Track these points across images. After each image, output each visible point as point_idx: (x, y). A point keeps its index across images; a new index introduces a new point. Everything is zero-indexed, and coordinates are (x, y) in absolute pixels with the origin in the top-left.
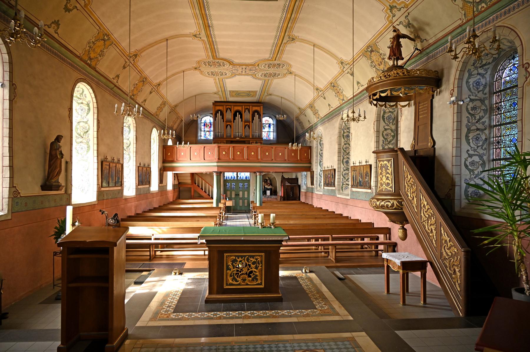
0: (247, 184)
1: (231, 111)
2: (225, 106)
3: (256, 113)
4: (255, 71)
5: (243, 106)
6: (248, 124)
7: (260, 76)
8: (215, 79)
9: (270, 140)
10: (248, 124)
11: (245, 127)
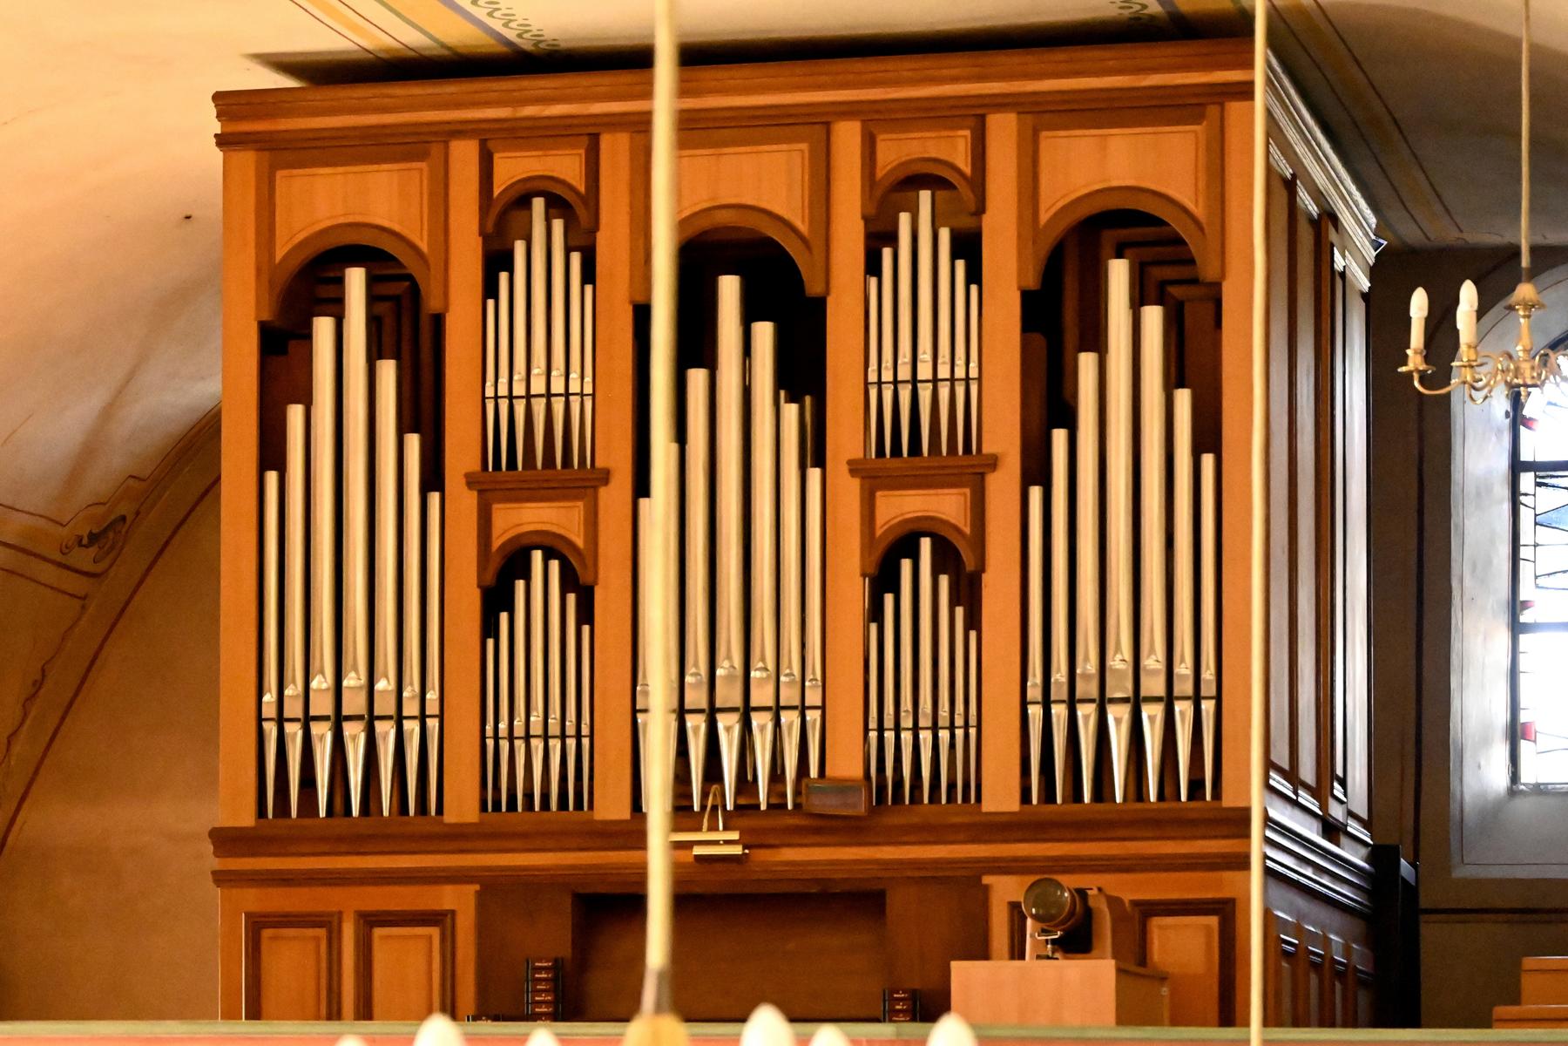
2: (465, 154)
5: (848, 136)
6: (948, 505)
10: (948, 505)
11: (883, 580)
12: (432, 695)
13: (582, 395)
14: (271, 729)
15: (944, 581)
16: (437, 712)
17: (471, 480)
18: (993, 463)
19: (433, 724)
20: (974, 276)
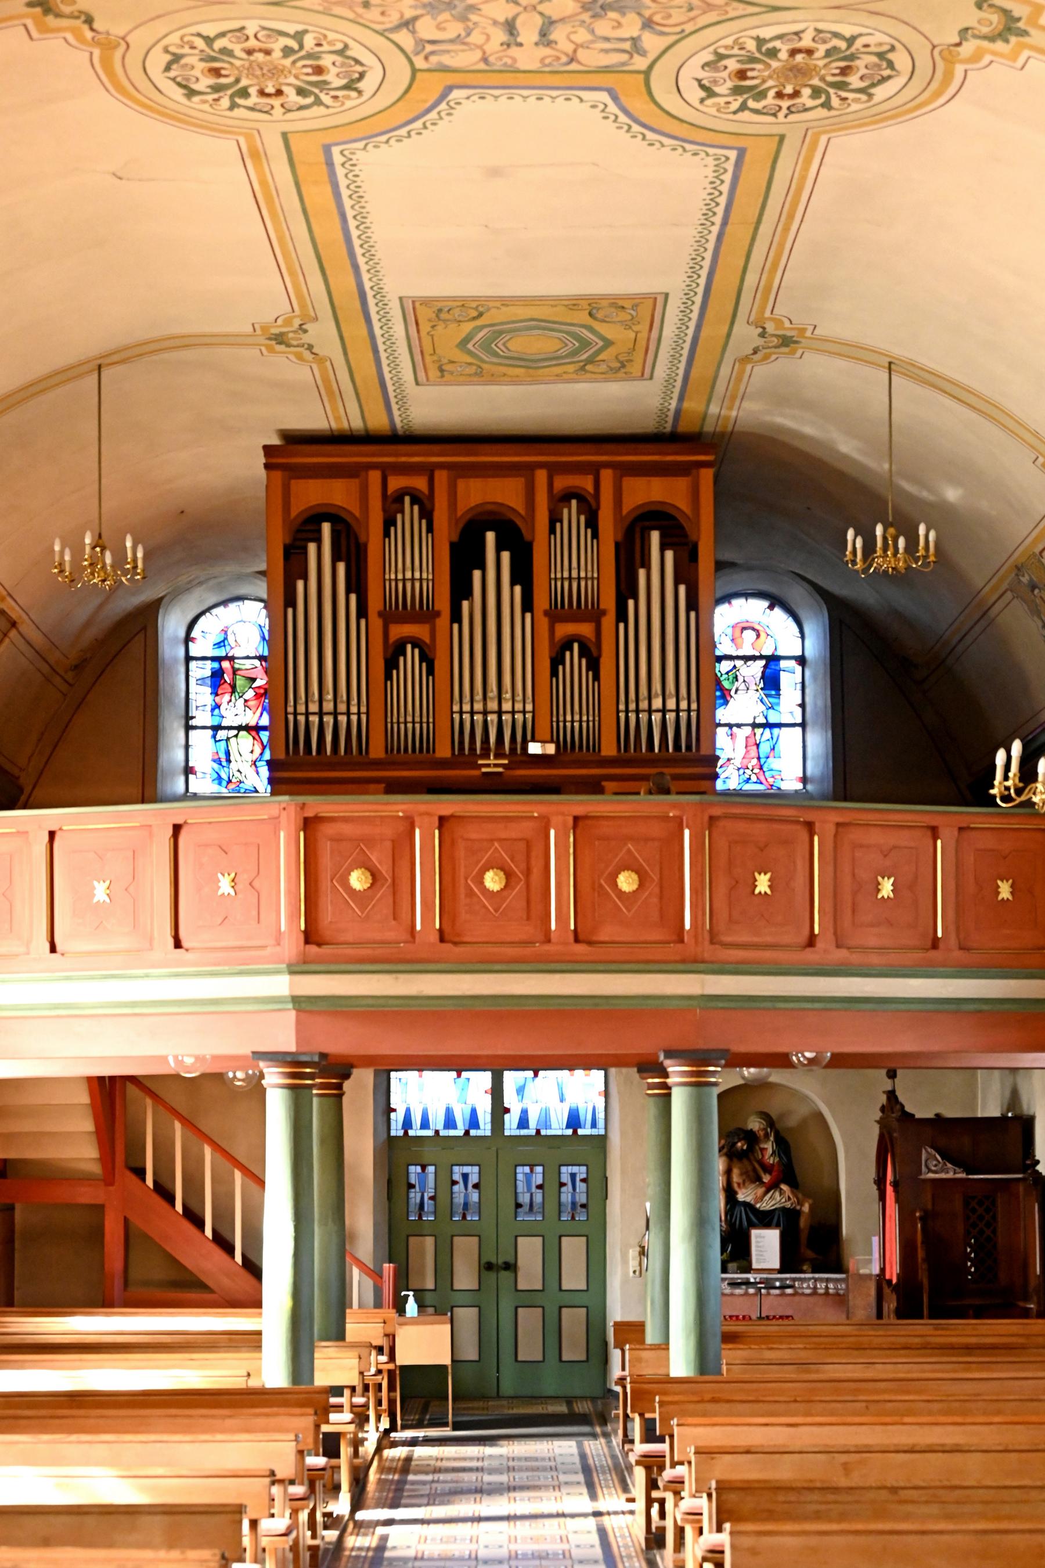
0: (581, 1171)
1: (427, 514)
2: (375, 476)
3: (655, 536)
4: (648, 24)
5: (541, 477)
6: (585, 629)
7: (694, 94)
8: (255, 155)
9: (776, 797)
10: (585, 629)
11: (557, 661)
13: (428, 580)
14: (291, 717)
15: (584, 661)
17: (380, 614)
18: (604, 613)
19: (364, 717)
20: (595, 535)
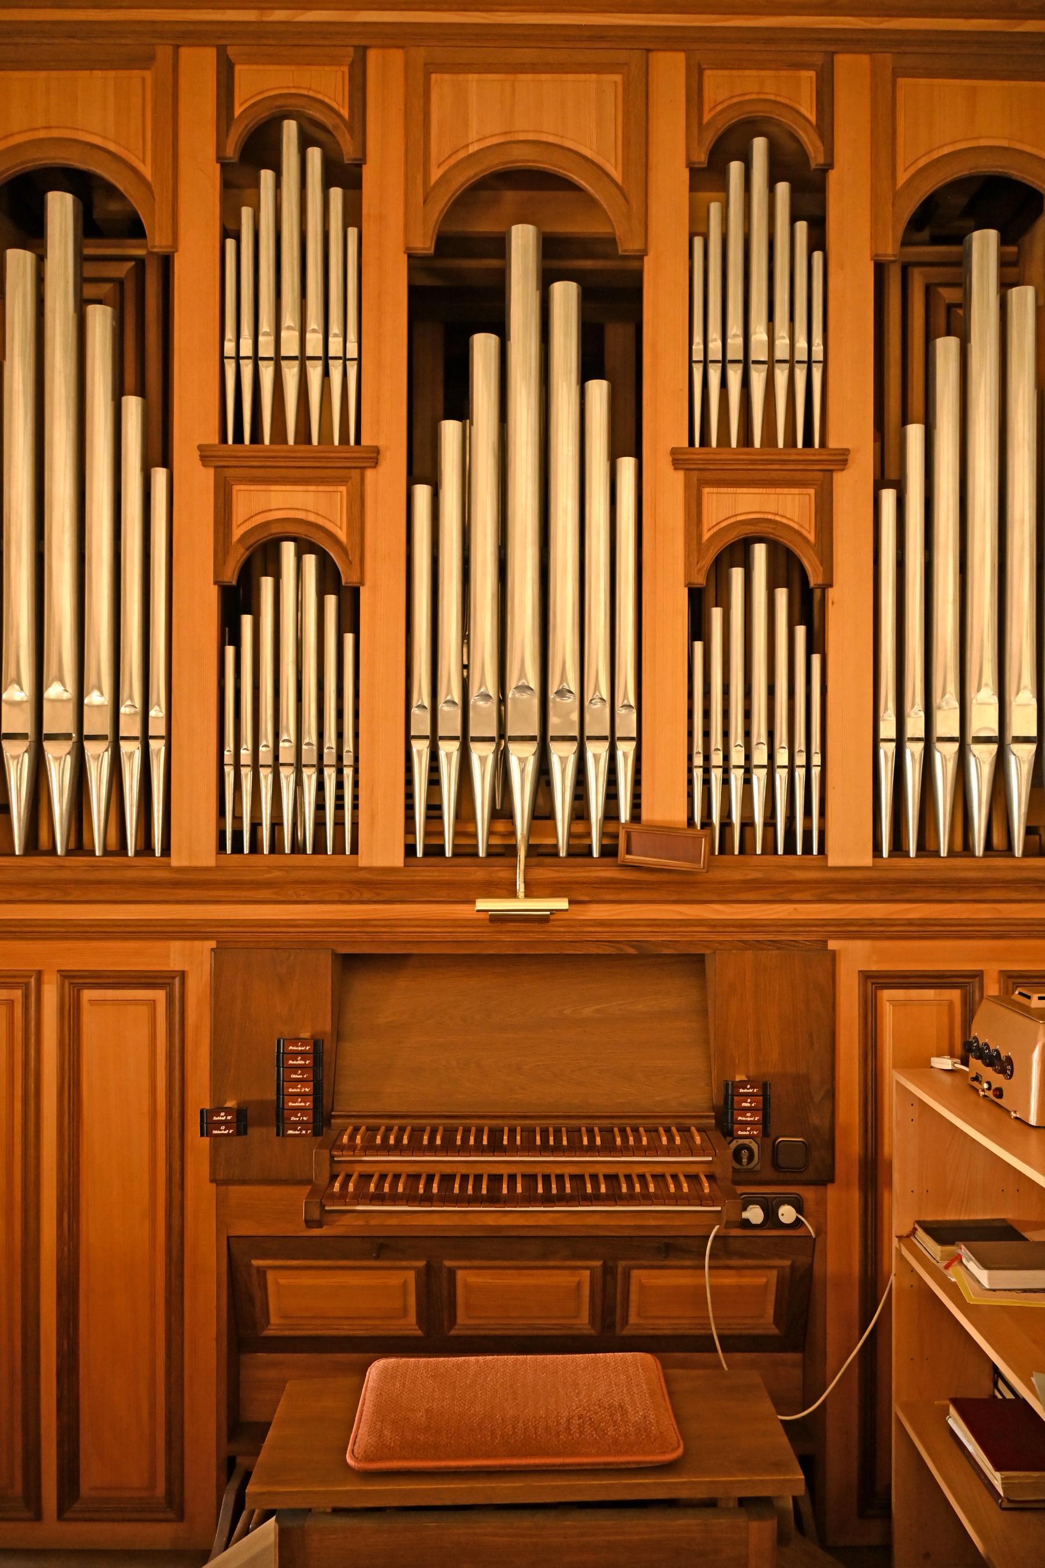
12: (157, 713)
16: (163, 732)
17: (206, 456)
18: (842, 459)
19: (157, 747)
20: (818, 241)
